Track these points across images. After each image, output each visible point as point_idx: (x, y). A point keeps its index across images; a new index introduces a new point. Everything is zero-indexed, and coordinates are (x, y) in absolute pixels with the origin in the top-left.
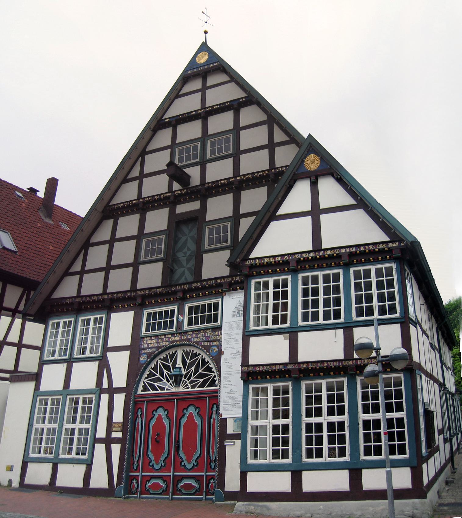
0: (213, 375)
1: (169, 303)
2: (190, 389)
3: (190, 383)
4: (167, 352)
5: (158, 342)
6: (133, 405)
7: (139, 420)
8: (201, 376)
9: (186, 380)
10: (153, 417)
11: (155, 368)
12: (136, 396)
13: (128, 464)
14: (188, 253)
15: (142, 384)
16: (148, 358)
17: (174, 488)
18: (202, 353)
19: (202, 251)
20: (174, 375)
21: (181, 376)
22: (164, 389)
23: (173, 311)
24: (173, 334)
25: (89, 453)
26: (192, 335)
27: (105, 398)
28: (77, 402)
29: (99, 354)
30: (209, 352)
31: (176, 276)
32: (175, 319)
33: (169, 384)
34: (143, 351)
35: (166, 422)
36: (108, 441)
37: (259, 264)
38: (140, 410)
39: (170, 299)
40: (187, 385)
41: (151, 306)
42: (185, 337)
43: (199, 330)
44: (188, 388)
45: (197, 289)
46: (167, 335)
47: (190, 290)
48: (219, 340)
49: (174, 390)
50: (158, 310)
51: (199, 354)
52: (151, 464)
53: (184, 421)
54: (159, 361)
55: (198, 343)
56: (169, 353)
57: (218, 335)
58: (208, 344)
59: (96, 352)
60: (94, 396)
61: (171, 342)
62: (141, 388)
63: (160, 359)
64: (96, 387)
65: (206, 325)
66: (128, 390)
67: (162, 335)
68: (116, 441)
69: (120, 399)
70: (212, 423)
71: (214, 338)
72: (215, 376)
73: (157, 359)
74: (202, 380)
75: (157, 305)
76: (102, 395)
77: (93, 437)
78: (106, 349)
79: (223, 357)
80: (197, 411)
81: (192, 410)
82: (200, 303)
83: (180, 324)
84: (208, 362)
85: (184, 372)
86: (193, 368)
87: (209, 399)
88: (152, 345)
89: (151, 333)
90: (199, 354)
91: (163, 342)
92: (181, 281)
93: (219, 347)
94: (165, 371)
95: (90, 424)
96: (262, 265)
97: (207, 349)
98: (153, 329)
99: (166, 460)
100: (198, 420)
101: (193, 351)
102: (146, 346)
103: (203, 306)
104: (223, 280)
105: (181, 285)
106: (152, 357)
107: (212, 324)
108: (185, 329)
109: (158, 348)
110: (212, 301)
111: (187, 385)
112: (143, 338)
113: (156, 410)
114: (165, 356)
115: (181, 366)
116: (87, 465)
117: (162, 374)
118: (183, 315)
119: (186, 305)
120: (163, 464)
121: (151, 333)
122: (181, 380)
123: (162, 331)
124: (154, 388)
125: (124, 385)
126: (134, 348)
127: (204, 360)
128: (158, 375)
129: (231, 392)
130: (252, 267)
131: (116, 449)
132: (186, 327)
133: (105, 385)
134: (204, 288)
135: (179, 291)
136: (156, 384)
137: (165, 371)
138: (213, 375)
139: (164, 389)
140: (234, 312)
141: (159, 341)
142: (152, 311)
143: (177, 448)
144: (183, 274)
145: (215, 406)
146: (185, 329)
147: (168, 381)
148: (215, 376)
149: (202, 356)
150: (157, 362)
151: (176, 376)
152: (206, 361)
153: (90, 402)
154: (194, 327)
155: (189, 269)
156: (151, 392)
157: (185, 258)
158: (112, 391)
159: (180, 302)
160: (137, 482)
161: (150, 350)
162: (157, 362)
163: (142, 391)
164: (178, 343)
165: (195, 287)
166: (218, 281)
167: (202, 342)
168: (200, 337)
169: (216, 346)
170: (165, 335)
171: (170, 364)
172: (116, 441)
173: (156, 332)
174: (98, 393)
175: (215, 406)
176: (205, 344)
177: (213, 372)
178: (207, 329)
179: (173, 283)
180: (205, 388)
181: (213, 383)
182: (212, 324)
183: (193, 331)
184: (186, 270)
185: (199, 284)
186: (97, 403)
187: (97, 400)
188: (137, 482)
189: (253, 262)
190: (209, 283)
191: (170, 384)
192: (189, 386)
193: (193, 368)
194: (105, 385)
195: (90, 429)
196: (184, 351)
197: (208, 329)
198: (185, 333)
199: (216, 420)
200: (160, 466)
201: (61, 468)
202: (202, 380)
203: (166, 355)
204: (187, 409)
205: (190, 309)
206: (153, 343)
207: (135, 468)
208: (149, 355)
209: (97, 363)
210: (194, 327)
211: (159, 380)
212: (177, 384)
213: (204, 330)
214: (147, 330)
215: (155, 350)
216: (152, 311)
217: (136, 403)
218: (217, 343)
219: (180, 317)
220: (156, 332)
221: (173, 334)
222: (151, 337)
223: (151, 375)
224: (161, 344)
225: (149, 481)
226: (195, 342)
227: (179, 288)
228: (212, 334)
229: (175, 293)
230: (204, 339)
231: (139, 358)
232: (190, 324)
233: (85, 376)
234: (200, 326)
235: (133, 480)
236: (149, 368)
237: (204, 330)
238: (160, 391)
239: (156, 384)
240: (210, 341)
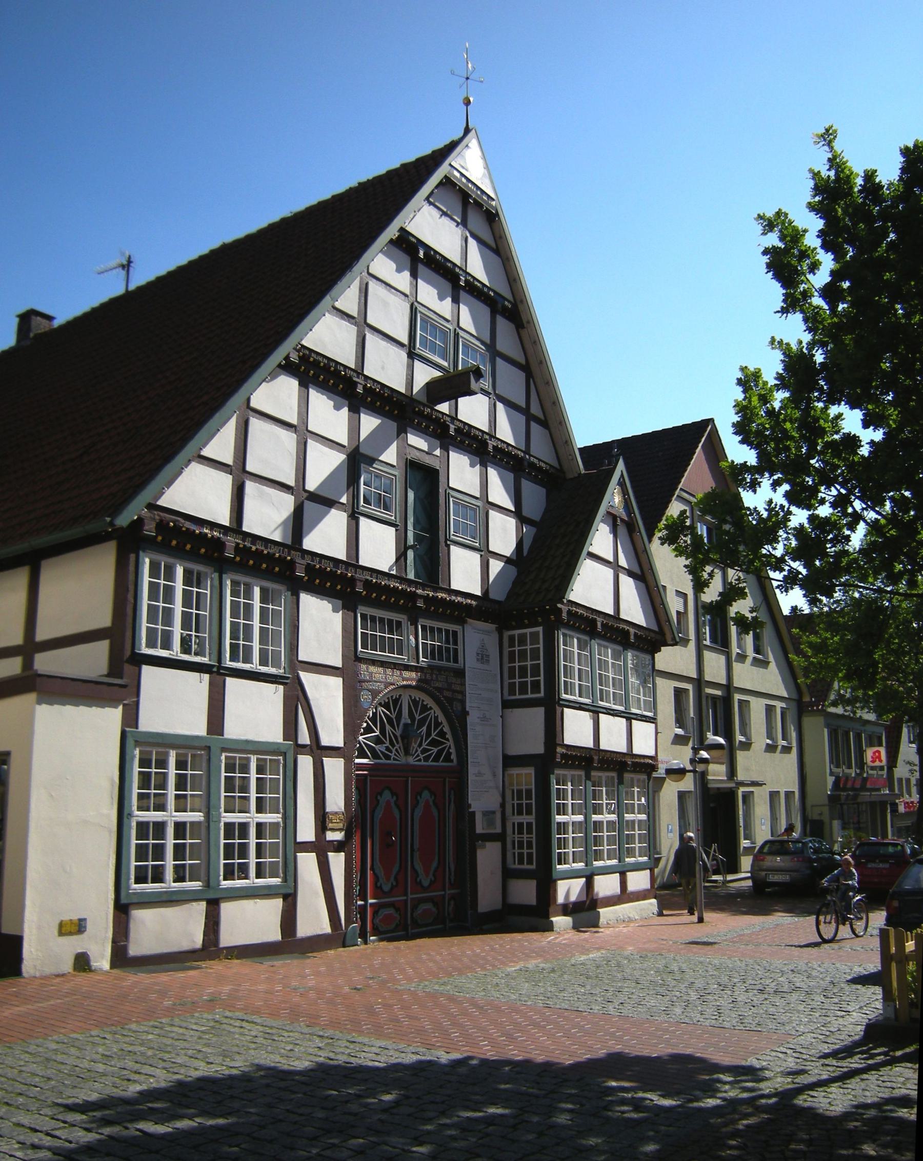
2: (422, 763)
8: (434, 743)
26: (431, 675)
36: (321, 848)
44: (420, 760)
48: (463, 693)
49: (403, 760)
51: (431, 708)
68: (338, 847)
72: (450, 747)
78: (296, 664)
79: (469, 719)
93: (463, 702)
94: (388, 727)
107: (451, 664)
116: (285, 897)
129: (479, 774)
133: (304, 737)
135: (421, 596)
137: (388, 727)
140: (478, 654)
176: (447, 693)
177: (448, 740)
181: (448, 759)
193: (425, 728)
194: (304, 737)
196: (410, 696)
201: (228, 909)
218: (460, 697)
226: (436, 688)
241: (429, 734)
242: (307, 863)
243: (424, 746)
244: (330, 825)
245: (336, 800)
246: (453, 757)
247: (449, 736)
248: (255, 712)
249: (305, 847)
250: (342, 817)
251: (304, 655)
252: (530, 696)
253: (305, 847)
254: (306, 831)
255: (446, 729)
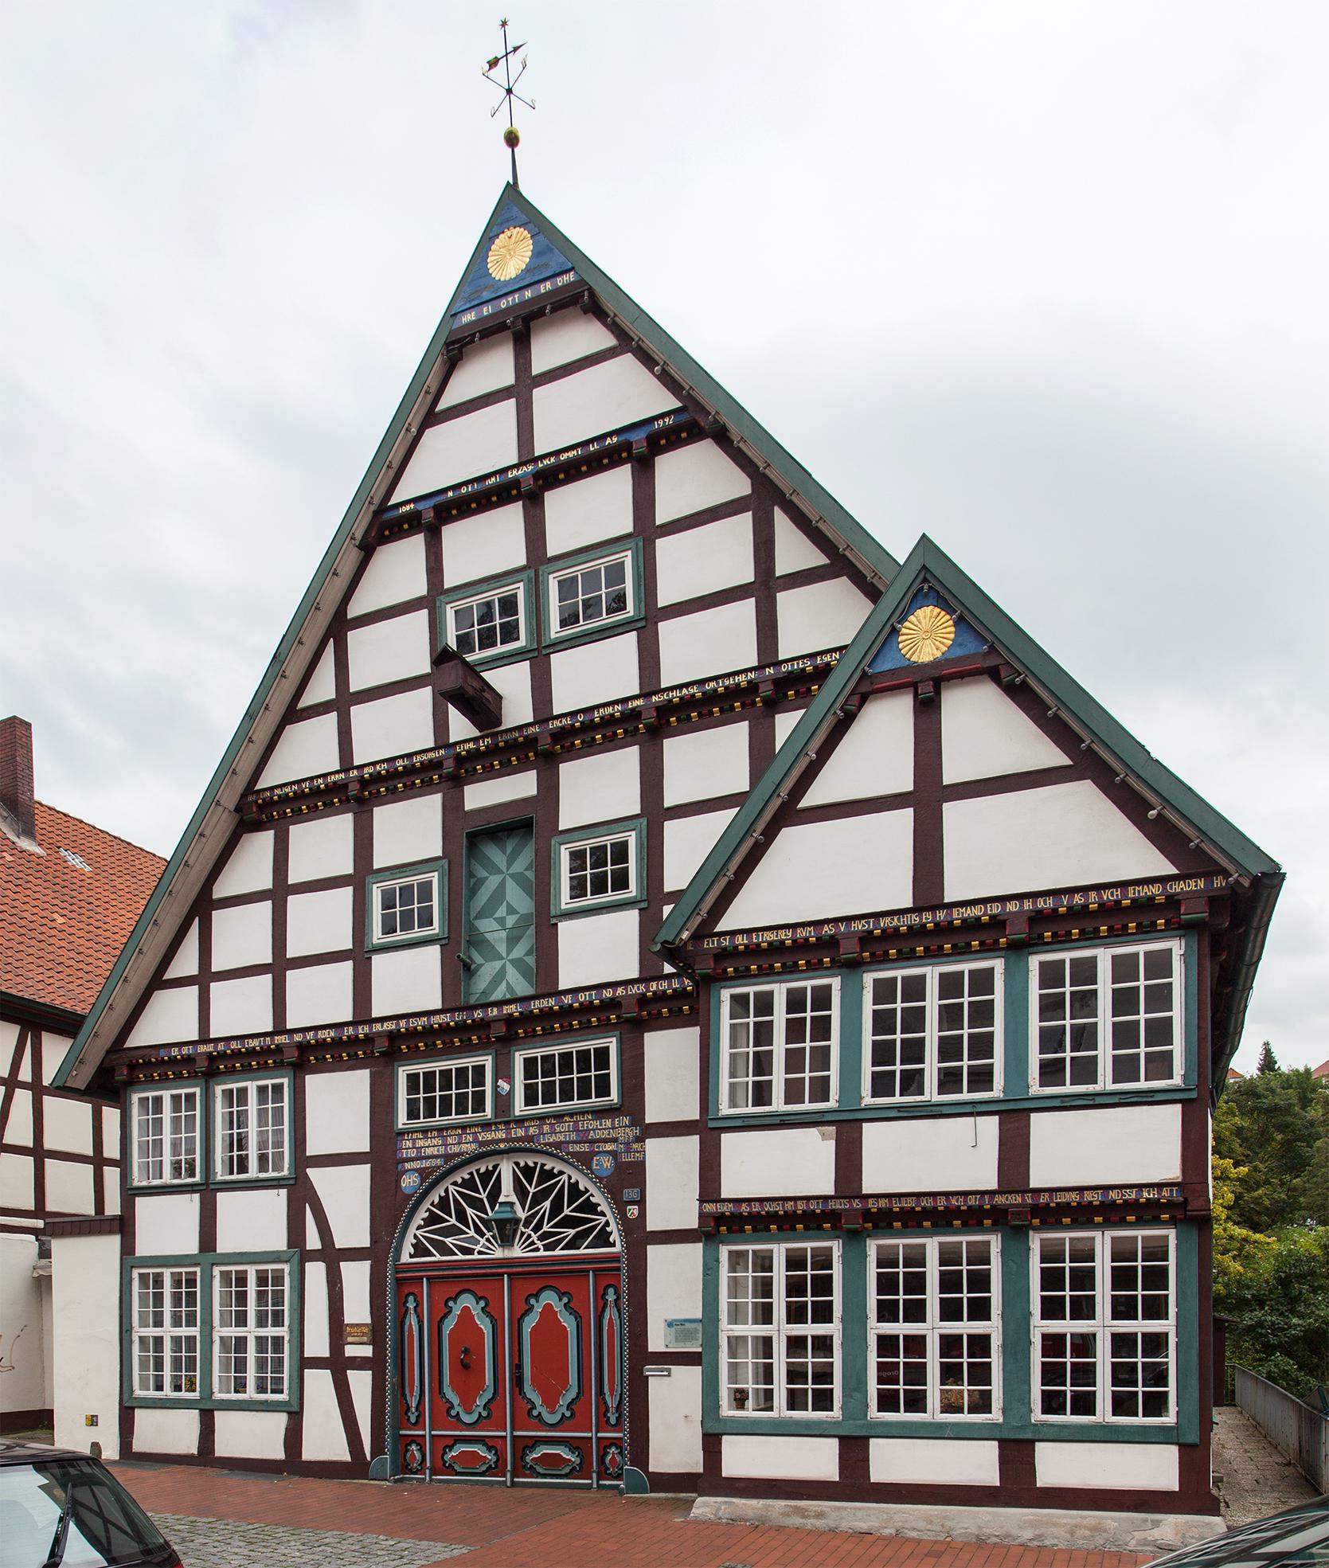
0: (603, 1220)
1: (467, 1049)
2: (542, 1253)
3: (540, 1238)
4: (473, 1168)
5: (446, 1145)
6: (394, 1288)
7: (412, 1319)
8: (568, 1222)
9: (529, 1231)
10: (449, 1312)
11: (444, 1204)
12: (399, 1268)
13: (393, 1411)
14: (511, 921)
15: (409, 1240)
16: (423, 1181)
17: (518, 1460)
18: (568, 1170)
19: (553, 913)
20: (497, 1221)
21: (517, 1221)
22: (470, 1251)
23: (479, 1070)
24: (486, 1126)
25: (290, 1388)
26: (540, 1127)
27: (316, 1272)
28: (242, 1280)
29: (286, 1172)
30: (589, 1168)
31: (482, 982)
32: (488, 1088)
33: (483, 1241)
34: (407, 1166)
35: (484, 1325)
36: (338, 1365)
37: (746, 946)
38: (411, 1298)
39: (470, 1040)
40: (533, 1243)
41: (415, 1056)
42: (521, 1133)
43: (559, 1117)
44: (537, 1249)
45: (547, 1015)
46: (470, 1126)
47: (528, 1018)
49: (499, 1253)
50: (437, 1066)
51: (561, 1173)
52: (453, 1413)
53: (530, 1323)
54: (451, 1188)
55: (557, 1145)
56: (478, 1171)
57: (613, 1128)
58: (585, 1148)
59: (278, 1167)
60: (286, 1268)
61: (482, 1144)
62: (408, 1248)
63: (455, 1183)
64: (290, 1246)
65: (576, 1103)
66: (378, 1252)
67: (456, 1128)
69: (357, 1277)
70: (606, 1328)
71: (605, 1134)
72: (607, 1224)
73: (447, 1183)
74: (572, 1232)
75: (432, 1054)
76: (310, 1267)
77: (296, 1356)
80: (565, 1300)
81: (549, 1298)
82: (556, 1050)
83: (503, 1103)
84: (587, 1190)
85: (522, 1214)
86: (547, 1204)
87: (595, 1276)
88: (429, 1151)
89: (422, 1122)
90: (561, 1173)
91: (459, 1143)
92: (499, 994)
94: (470, 1211)
95: (286, 1328)
96: (753, 951)
97: (584, 1161)
98: (430, 1113)
99: (491, 1406)
100: (568, 1322)
101: (543, 1165)
102: (413, 1154)
103: (566, 1057)
104: (620, 991)
105: (499, 1004)
106: (431, 1179)
107: (594, 1101)
108: (517, 1113)
109: (447, 1157)
110: (591, 1045)
111: (533, 1243)
112: (402, 1133)
113: (455, 1299)
114: (467, 1177)
115: (513, 1198)
117: (462, 1217)
118: (510, 1079)
119: (517, 1054)
120: (484, 1414)
121: (422, 1122)
122: (515, 1231)
123: (454, 1118)
124: (444, 1249)
125: (365, 1241)
126: (383, 1155)
127: (574, 1187)
128: (453, 1221)
130: (723, 955)
131: (361, 1383)
132: (519, 1107)
133: (313, 1241)
134: (567, 1012)
135: (496, 1020)
136: (448, 1241)
137: (470, 1211)
138: (603, 1220)
139: (470, 1251)
141: (450, 1140)
142: (421, 1068)
143: (518, 1381)
144: (501, 975)
145: (611, 1291)
146: (517, 1113)
147: (482, 1235)
148: (607, 1224)
149: (570, 1178)
150: (447, 1191)
151: (501, 1224)
152: (581, 1188)
153: (278, 1279)
154: (541, 1108)
155: (518, 964)
156: (438, 1257)
157: (503, 934)
158: (333, 1256)
159: (498, 1046)
160: (422, 1450)
161: (425, 1164)
162: (447, 1191)
163: (411, 1256)
164: (502, 1146)
165: (541, 1010)
166: (608, 994)
167: (568, 1143)
168: (563, 1132)
169: (609, 1153)
170: (464, 1127)
171: (483, 1196)
172: (359, 1363)
173: (439, 1120)
174: (296, 1259)
175: (611, 1291)
176: (577, 1148)
177: (603, 1214)
178: (583, 1113)
179: (473, 1001)
180: (582, 1251)
181: (603, 1239)
182: (594, 1101)
183: (542, 1118)
184: (509, 965)
185: (552, 1002)
186: (296, 1283)
187: (296, 1276)
188: (422, 1450)
189: (726, 942)
190: (582, 997)
191: (488, 1240)
192: (539, 1244)
193: (547, 1204)
194: (313, 1241)
195: (286, 1339)
196: (517, 1164)
197: (583, 1113)
198: (520, 1121)
199: (616, 1323)
200: (475, 1417)
202: (572, 1232)
203: (471, 1174)
204: (537, 1296)
205: (530, 1063)
206: (432, 1146)
207: (413, 1420)
208: (423, 1173)
209: (284, 1192)
210: (541, 1108)
211: (452, 1231)
212: (506, 1240)
213: (571, 1115)
214: (412, 1114)
215: (439, 1162)
216: (421, 1068)
217: (399, 1282)
218: (609, 1147)
219: (500, 1082)
220: (439, 1120)
221: (486, 1126)
222: (425, 1131)
223: (432, 1219)
224: (456, 1149)
225: (451, 1447)
226: (550, 1145)
227: (494, 1012)
228: (595, 1124)
229: (483, 1025)
230: (574, 1137)
231: (398, 1182)
232: (530, 1100)
233: (254, 1222)
234: (558, 1106)
235: (410, 1444)
236: (426, 1205)
237: (571, 1114)
238: (460, 1257)
239: (448, 1241)
240: (592, 1142)
241: (557, 1208)
242: (319, 1382)
243: (545, 1228)
244: (350, 1339)
245: (358, 1309)
246: (615, 1237)
247: (603, 1207)
248: (254, 1222)
249: (317, 1363)
250: (366, 1330)
251: (311, 1150)
252: (807, 1106)
253: (317, 1363)
254: (317, 1344)
255: (597, 1198)
